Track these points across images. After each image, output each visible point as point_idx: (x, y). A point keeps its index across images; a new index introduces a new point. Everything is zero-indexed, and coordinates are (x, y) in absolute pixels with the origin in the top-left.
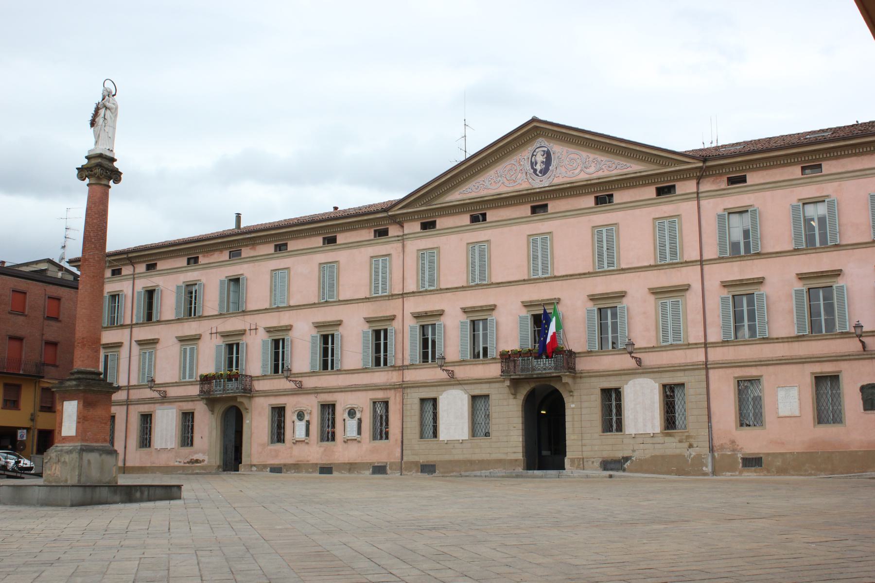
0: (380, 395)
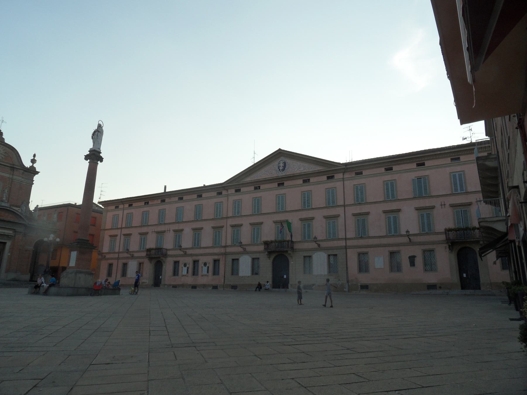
0: (216, 257)
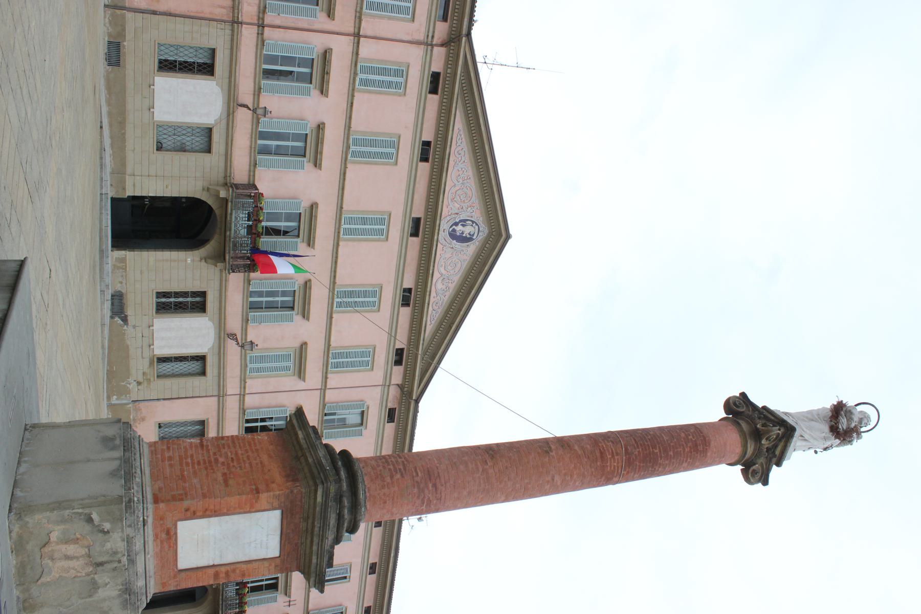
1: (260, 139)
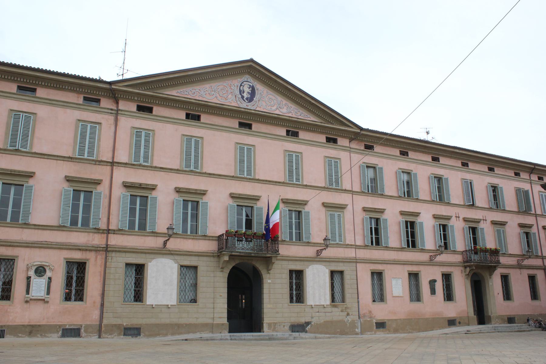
0: (77, 256)
1: (187, 233)
